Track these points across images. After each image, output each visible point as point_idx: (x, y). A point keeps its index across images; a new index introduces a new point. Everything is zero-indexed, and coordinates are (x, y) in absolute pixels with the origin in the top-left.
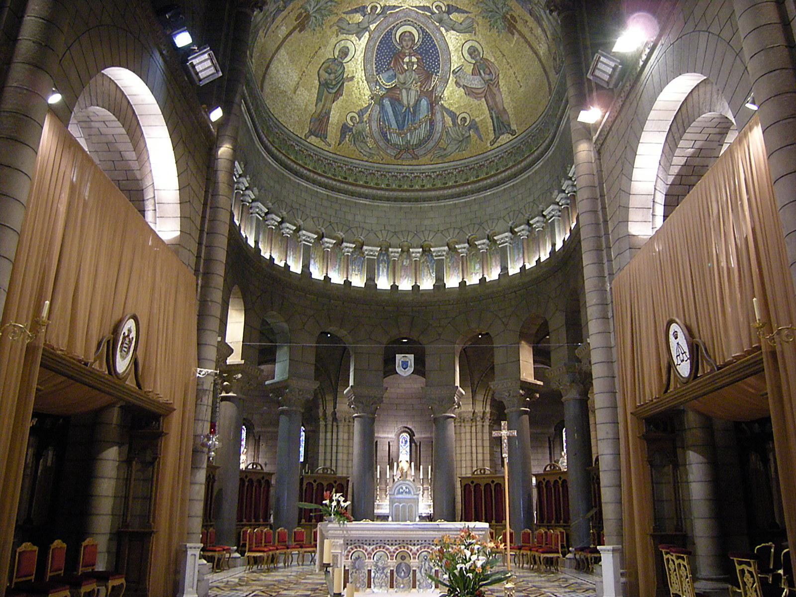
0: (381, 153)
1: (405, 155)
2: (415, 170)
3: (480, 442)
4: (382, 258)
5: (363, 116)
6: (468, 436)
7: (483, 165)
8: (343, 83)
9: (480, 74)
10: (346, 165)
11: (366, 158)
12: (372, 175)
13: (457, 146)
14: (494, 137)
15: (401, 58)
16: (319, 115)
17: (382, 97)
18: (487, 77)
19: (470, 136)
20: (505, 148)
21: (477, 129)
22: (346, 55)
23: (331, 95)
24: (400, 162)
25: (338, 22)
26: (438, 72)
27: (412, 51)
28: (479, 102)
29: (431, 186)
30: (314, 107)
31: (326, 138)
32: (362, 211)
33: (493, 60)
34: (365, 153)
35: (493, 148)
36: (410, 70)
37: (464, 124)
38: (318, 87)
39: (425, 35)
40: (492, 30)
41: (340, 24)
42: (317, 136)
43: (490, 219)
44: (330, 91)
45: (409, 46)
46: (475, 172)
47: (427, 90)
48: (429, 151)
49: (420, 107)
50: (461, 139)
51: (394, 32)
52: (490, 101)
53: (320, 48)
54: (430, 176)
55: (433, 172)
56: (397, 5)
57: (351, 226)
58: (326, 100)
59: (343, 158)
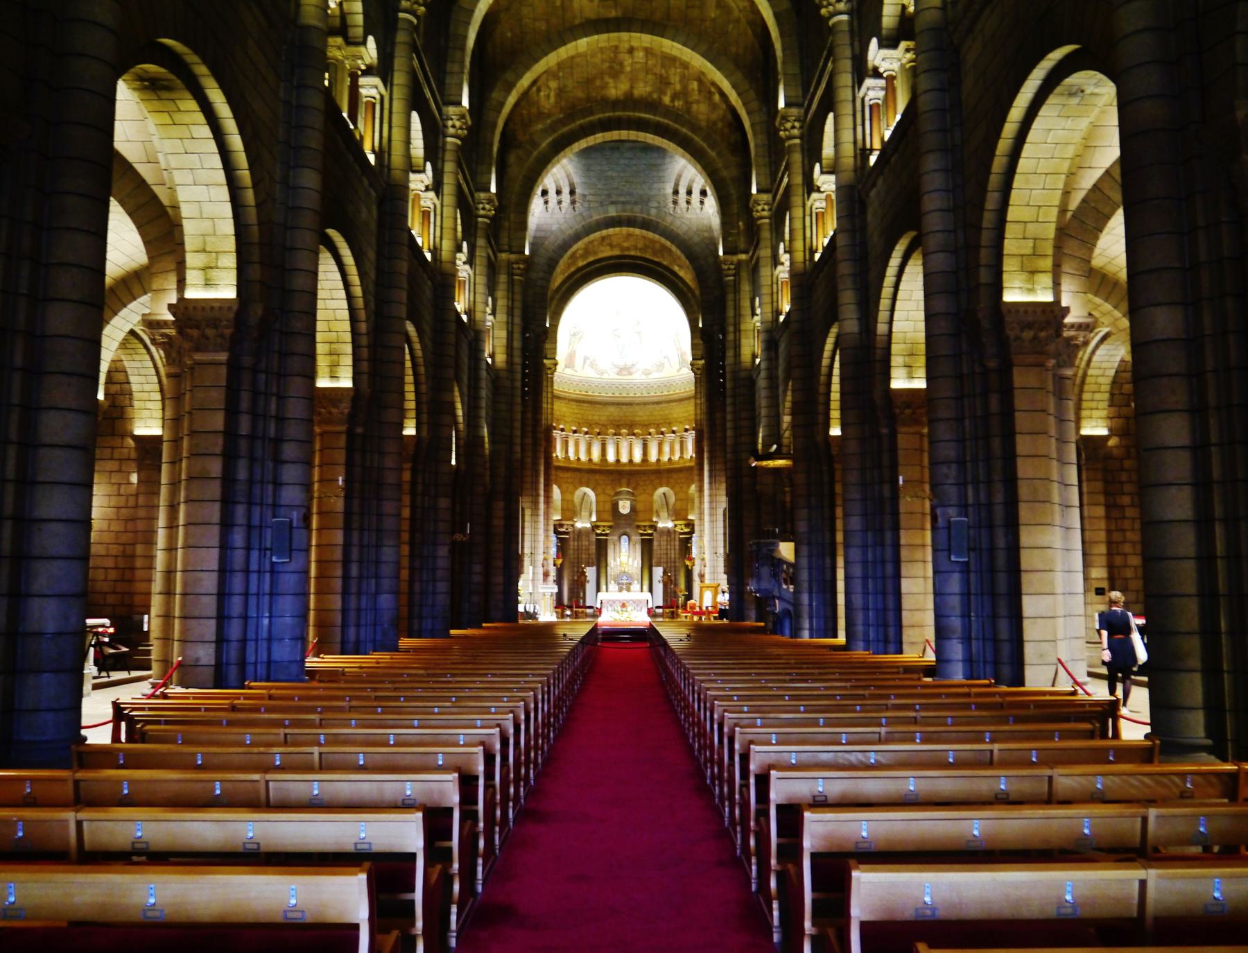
1: (624, 373)
3: (673, 547)
6: (665, 543)
11: (599, 376)
24: (620, 377)
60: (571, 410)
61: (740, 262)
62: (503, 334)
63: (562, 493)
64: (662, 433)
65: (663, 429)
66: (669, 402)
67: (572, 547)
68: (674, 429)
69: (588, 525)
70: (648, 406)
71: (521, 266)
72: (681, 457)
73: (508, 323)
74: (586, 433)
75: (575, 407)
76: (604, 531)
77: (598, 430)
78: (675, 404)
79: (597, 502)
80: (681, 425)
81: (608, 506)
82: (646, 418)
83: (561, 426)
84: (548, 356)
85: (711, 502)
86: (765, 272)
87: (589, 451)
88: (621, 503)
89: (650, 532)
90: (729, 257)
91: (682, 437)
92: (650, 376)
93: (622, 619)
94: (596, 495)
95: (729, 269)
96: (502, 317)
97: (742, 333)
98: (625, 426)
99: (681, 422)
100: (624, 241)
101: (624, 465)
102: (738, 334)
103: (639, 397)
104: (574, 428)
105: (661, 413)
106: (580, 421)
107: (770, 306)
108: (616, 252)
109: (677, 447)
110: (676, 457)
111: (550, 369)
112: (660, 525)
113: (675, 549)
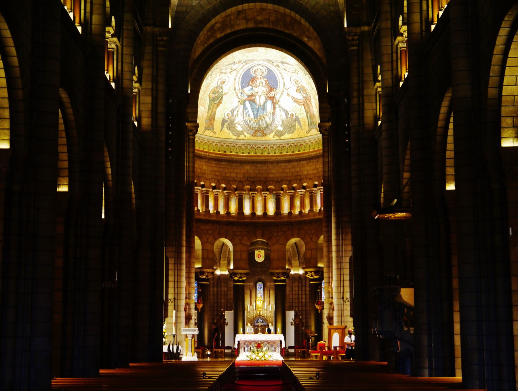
0: (245, 133)
1: (259, 134)
2: (265, 143)
3: (304, 292)
4: (246, 196)
5: (233, 112)
6: (297, 289)
7: (302, 145)
8: (222, 97)
9: (301, 93)
10: (225, 143)
11: (235, 138)
12: (240, 148)
13: (288, 130)
14: (308, 129)
15: (255, 80)
16: (210, 117)
17: (245, 101)
18: (305, 95)
19: (295, 125)
20: (314, 138)
21: (299, 122)
22: (224, 82)
23: (216, 104)
24: (255, 138)
25: (220, 71)
26: (277, 88)
27: (262, 77)
28: (300, 107)
29: (273, 153)
30: (207, 114)
31: (214, 129)
32: (235, 171)
33: (307, 88)
34: (235, 134)
35: (308, 135)
36: (261, 86)
37: (292, 118)
38: (209, 102)
39: (269, 71)
40: (306, 76)
41: (221, 71)
42: (209, 130)
43: (305, 178)
44: (216, 102)
45: (260, 75)
46: (298, 148)
47: (271, 96)
48: (272, 132)
49: (267, 105)
50: (291, 126)
51: (251, 69)
52: (306, 108)
53: (210, 84)
54: (273, 147)
55: (275, 145)
56: (252, 59)
57: (229, 180)
58: (213, 108)
59: (223, 140)
60: (211, 168)
61: (362, 32)
62: (149, 99)
63: (203, 244)
64: (294, 189)
65: (295, 185)
66: (300, 160)
67: (211, 293)
68: (305, 184)
69: (227, 273)
70: (280, 164)
71: (165, 38)
72: (311, 210)
73: (152, 89)
74: (225, 189)
75: (214, 165)
76: (241, 277)
77: (235, 186)
78: (304, 162)
79: (234, 251)
80: (311, 181)
81: (245, 256)
82: (278, 175)
83: (202, 183)
84: (190, 120)
85: (338, 251)
86: (386, 42)
87: (227, 206)
88: (256, 252)
89: (283, 278)
90: (351, 29)
91: (311, 192)
92: (282, 138)
93: (258, 358)
94: (234, 246)
95: (353, 40)
96: (147, 84)
97: (366, 98)
98: (260, 182)
99: (310, 179)
100: (258, 15)
101: (259, 217)
102: (361, 98)
103: (272, 156)
104: (213, 184)
105: (293, 171)
106: (219, 178)
107: (390, 73)
108: (251, 25)
109: (307, 201)
110: (307, 210)
111: (191, 131)
112: (292, 272)
113: (306, 294)
